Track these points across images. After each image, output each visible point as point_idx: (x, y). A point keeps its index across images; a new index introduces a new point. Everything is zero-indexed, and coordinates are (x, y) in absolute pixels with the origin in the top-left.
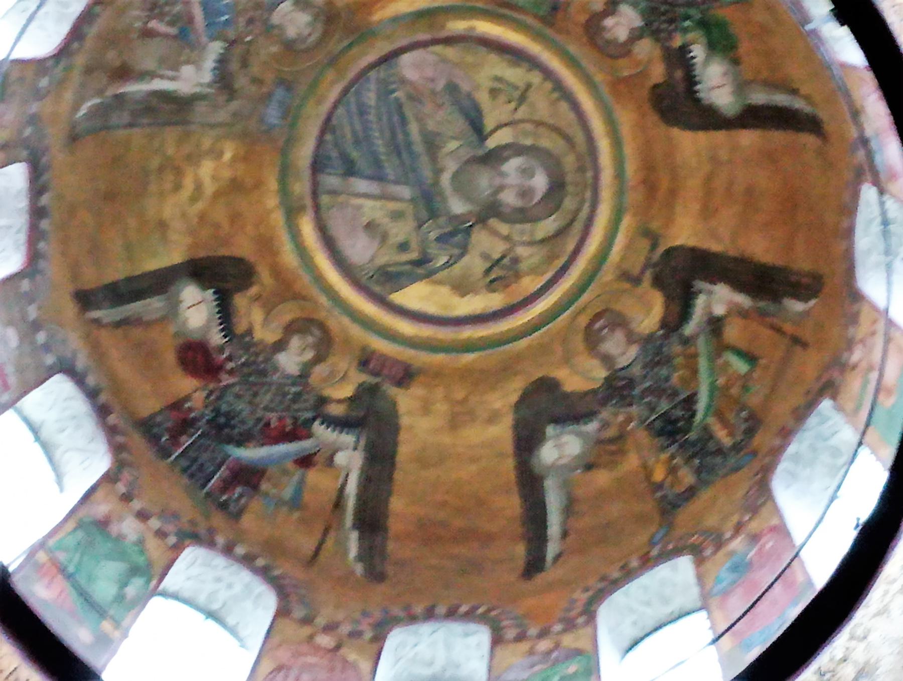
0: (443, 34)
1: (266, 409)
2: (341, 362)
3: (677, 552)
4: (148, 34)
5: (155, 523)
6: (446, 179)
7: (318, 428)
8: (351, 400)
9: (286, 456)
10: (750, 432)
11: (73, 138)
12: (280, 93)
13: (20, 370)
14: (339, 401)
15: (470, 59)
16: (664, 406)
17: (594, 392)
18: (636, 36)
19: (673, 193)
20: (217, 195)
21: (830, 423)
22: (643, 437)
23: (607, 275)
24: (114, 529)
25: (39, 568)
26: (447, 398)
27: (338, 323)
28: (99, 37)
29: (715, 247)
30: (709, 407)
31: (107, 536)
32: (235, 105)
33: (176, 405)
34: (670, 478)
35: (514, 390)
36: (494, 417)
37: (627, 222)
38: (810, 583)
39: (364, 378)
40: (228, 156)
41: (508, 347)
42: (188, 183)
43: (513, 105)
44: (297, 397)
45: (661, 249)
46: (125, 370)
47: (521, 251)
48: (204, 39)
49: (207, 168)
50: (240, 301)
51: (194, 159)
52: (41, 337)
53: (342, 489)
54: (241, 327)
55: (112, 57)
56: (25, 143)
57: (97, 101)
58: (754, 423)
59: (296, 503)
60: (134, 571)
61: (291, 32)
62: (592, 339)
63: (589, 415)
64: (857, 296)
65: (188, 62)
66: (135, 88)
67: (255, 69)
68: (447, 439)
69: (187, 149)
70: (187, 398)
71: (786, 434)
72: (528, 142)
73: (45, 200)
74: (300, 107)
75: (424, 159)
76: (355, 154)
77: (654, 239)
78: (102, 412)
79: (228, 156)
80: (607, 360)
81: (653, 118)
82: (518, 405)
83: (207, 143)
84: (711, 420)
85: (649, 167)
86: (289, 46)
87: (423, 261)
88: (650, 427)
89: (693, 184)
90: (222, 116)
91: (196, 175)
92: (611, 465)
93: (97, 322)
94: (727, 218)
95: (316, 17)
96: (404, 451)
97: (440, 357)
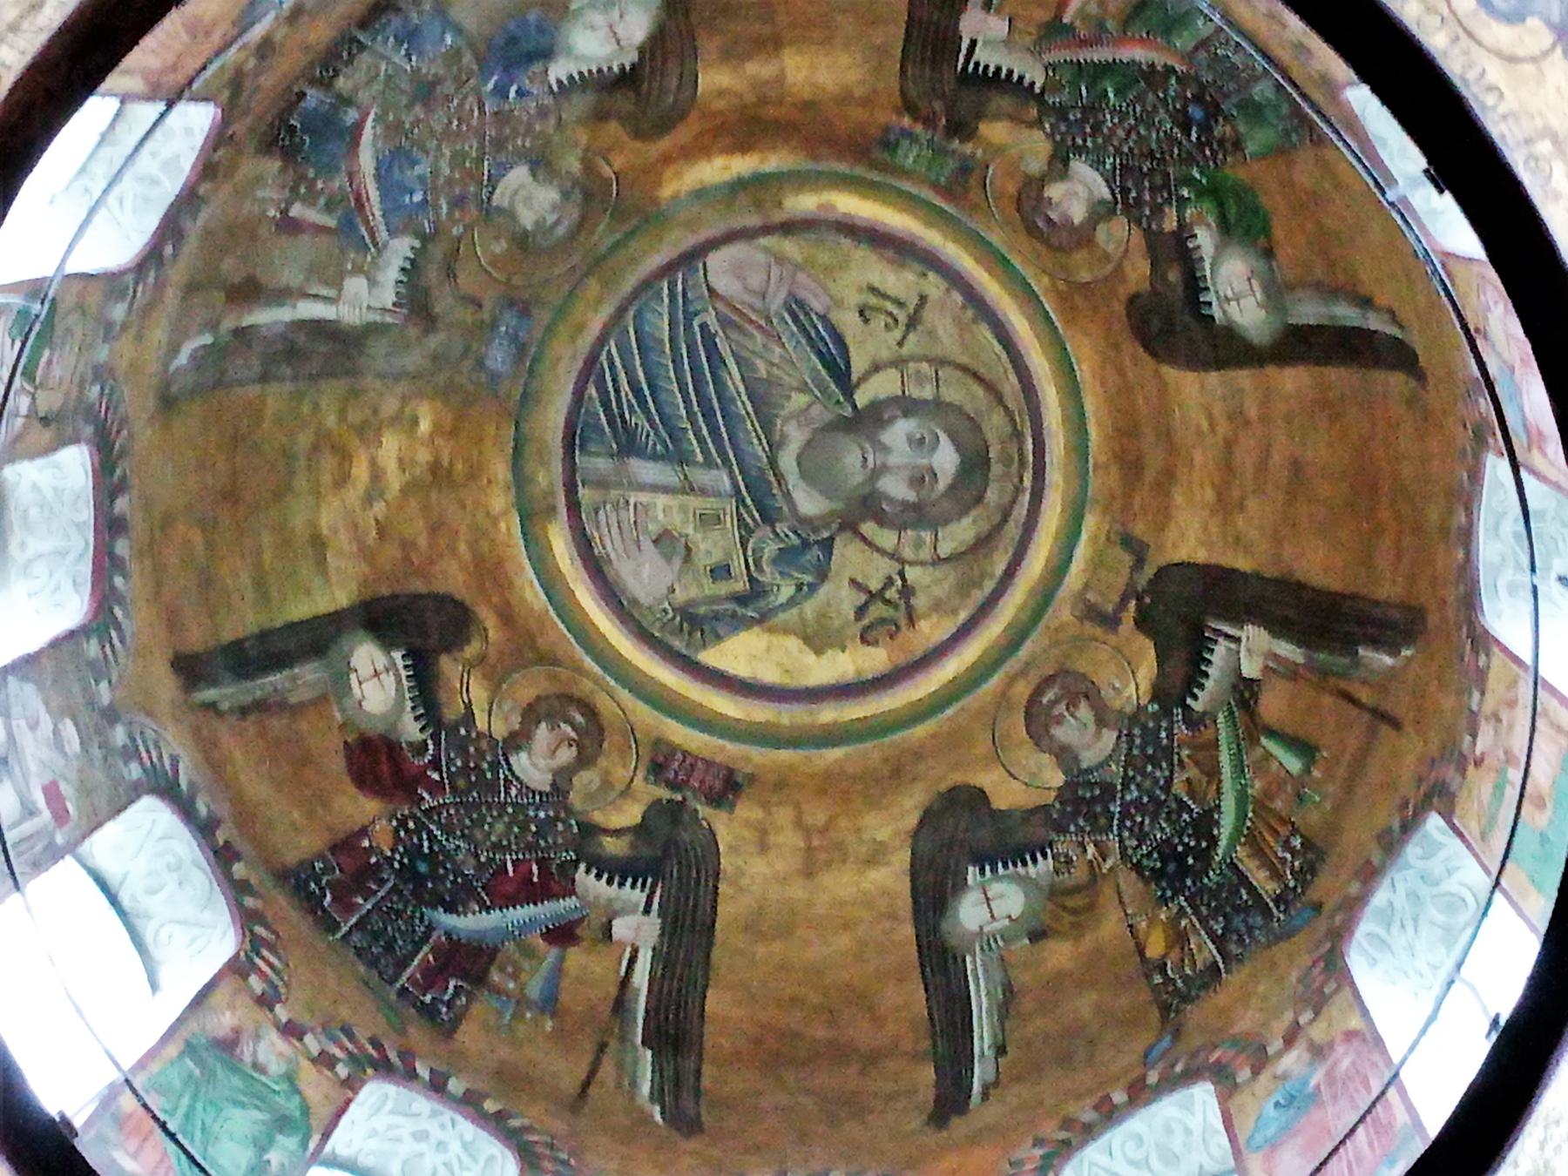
0: (778, 217)
1: (497, 847)
2: (619, 766)
3: (1190, 1076)
4: (289, 226)
5: (312, 1043)
6: (787, 461)
7: (585, 879)
8: (641, 831)
9: (525, 927)
10: (1307, 874)
11: (168, 402)
12: (508, 321)
13: (85, 790)
14: (617, 833)
15: (824, 257)
16: (1162, 831)
17: (1044, 809)
18: (1100, 213)
19: (1168, 476)
20: (406, 490)
21: (1442, 854)
22: (1129, 882)
23: (1063, 612)
24: (246, 1051)
25: (121, 1122)
26: (799, 823)
27: (616, 702)
28: (208, 234)
29: (1243, 564)
30: (1237, 830)
31: (235, 1067)
32: (434, 341)
33: (346, 845)
34: (1175, 954)
35: (909, 806)
36: (877, 855)
37: (1091, 523)
38: (1417, 1124)
39: (664, 793)
40: (425, 426)
41: (898, 736)
42: (361, 471)
43: (897, 334)
44: (546, 827)
45: (1149, 571)
46: (257, 787)
47: (912, 574)
48: (383, 235)
49: (390, 446)
50: (449, 667)
51: (369, 432)
52: (119, 735)
53: (625, 982)
54: (452, 711)
55: (231, 268)
56: (90, 413)
57: (207, 339)
58: (1313, 856)
59: (550, 1003)
60: (282, 1123)
61: (527, 219)
62: (1038, 722)
63: (1038, 849)
64: (1482, 640)
65: (358, 270)
66: (267, 317)
67: (467, 280)
68: (797, 891)
69: (355, 416)
70: (364, 832)
71: (1370, 875)
72: (927, 393)
73: (121, 504)
74: (542, 344)
75: (751, 426)
76: (637, 419)
77: (1138, 551)
78: (222, 857)
79: (425, 426)
80: (1065, 755)
81: (1132, 350)
82: (916, 834)
83: (390, 406)
84: (1241, 852)
85: (1125, 432)
86: (523, 242)
87: (756, 591)
88: (1138, 868)
89: (1202, 458)
90: (413, 360)
91: (373, 463)
92: (1077, 931)
93: (211, 706)
94: (1256, 518)
95: (566, 195)
96: (729, 910)
97: (785, 755)
